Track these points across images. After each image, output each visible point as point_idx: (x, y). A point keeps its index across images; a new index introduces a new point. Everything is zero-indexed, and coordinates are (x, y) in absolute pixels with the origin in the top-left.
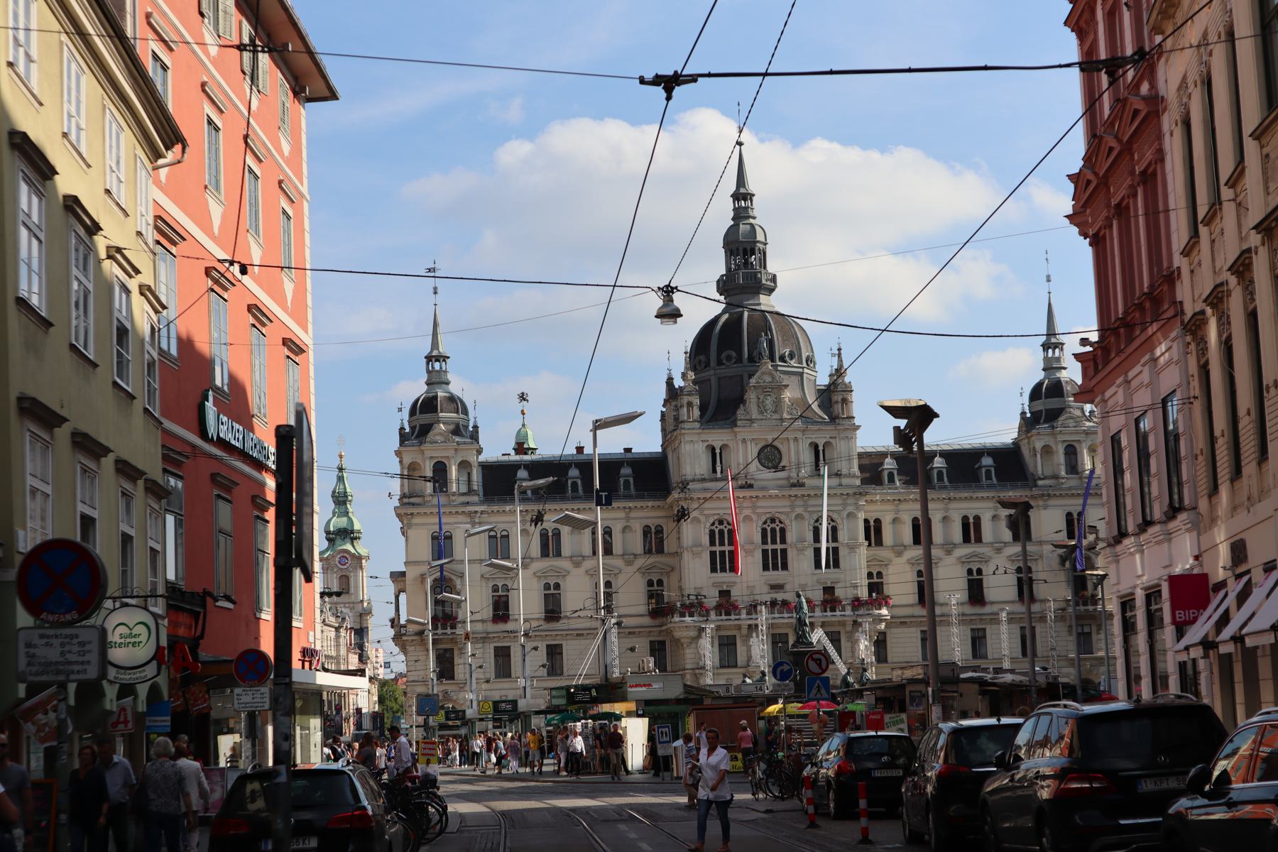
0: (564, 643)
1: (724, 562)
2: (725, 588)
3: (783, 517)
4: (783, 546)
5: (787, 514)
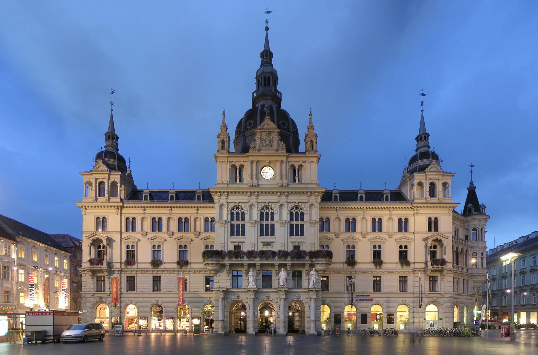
0: (162, 275)
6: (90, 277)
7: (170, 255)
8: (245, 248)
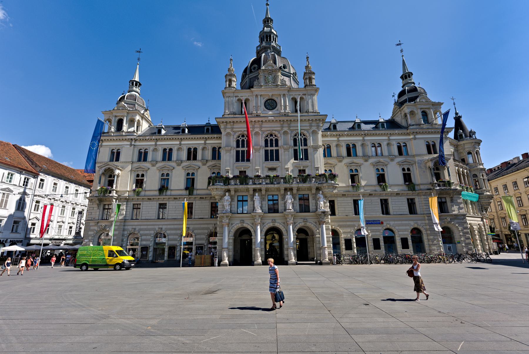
0: (167, 202)
1: (243, 157)
2: (242, 170)
3: (276, 133)
4: (276, 148)
5: (279, 131)
6: (96, 206)
7: (177, 182)
8: (250, 174)
